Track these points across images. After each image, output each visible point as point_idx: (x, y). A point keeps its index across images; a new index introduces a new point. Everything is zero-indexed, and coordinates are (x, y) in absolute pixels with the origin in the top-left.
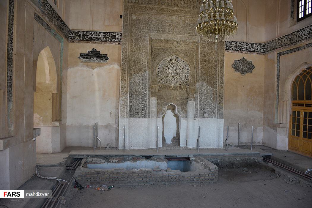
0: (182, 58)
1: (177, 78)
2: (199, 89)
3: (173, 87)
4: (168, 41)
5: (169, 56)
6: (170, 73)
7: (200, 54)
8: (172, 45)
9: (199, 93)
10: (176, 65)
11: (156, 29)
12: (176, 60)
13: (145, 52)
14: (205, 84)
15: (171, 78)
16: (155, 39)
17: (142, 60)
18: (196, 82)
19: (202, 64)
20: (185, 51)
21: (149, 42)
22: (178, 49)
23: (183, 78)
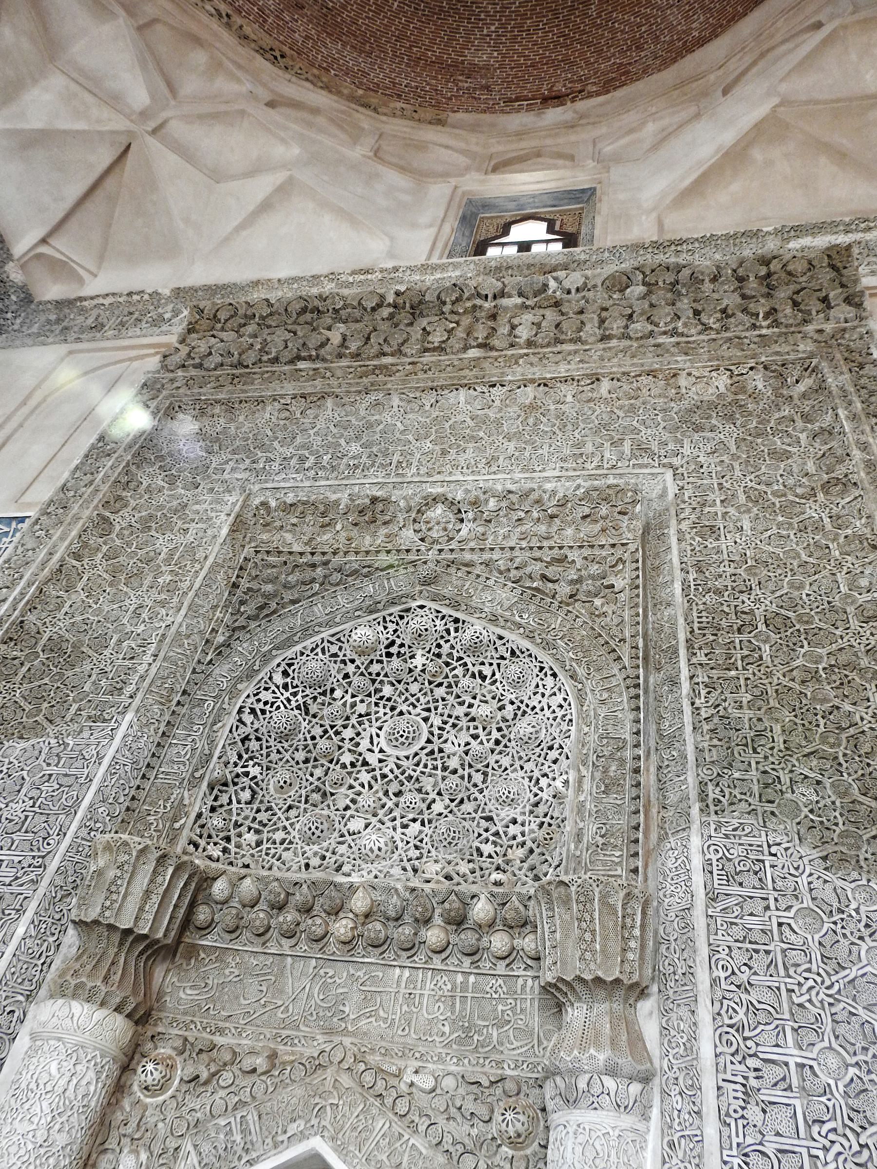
0: (494, 619)
1: (438, 807)
2: (699, 921)
3: (359, 903)
4: (380, 506)
5: (371, 612)
6: (372, 759)
7: (678, 574)
8: (408, 537)
9: (703, 978)
10: (440, 692)
11: (307, 465)
13: (171, 588)
14: (795, 860)
15: (367, 799)
16: (273, 504)
17: (120, 642)
18: (663, 838)
19: (711, 645)
20: (528, 570)
21: (225, 531)
22: (467, 556)
23: (507, 813)
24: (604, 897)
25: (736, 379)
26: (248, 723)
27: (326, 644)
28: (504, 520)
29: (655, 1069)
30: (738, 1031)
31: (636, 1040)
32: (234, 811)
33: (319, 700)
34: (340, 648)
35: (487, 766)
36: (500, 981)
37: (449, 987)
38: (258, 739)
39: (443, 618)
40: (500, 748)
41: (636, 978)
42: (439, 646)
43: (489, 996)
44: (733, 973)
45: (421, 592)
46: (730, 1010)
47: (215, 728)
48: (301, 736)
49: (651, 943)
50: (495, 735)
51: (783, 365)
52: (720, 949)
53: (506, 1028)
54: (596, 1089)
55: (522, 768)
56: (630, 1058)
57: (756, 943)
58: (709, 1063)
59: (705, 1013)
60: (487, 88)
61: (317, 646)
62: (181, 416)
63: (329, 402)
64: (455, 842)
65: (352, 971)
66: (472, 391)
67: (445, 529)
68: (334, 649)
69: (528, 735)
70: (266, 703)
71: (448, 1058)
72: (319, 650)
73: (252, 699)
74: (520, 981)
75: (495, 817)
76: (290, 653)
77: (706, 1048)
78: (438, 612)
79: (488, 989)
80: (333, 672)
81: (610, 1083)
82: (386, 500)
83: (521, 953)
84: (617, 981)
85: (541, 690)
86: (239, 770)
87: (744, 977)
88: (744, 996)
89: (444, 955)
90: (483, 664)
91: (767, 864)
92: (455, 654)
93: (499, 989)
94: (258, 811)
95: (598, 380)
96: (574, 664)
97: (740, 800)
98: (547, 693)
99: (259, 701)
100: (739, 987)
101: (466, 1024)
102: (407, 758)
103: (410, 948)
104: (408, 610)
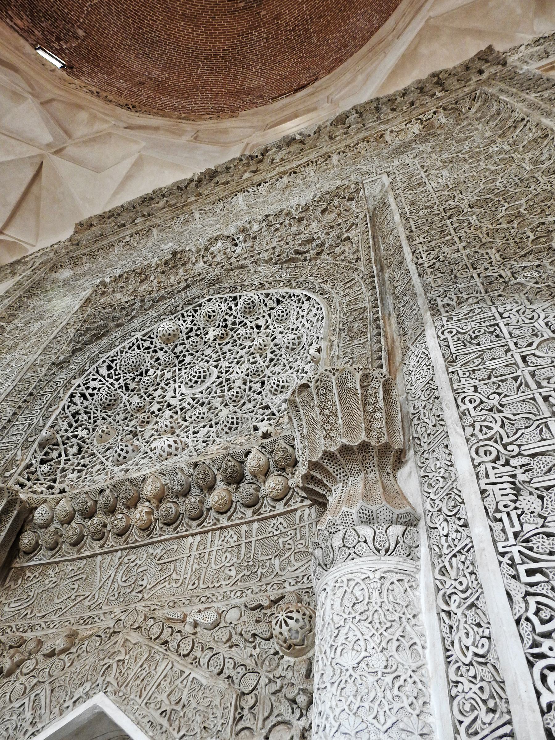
2: (442, 380)
4: (179, 256)
12: (230, 320)
24: (342, 384)
25: (425, 123)
26: (79, 404)
27: (140, 342)
28: (266, 234)
29: (420, 515)
30: (496, 442)
31: (394, 495)
32: (63, 462)
33: (137, 380)
34: (152, 343)
35: (264, 377)
36: (281, 520)
37: (235, 538)
38: (86, 413)
39: (226, 300)
40: (275, 362)
41: (385, 439)
42: (225, 320)
43: (271, 534)
44: (482, 402)
45: (209, 291)
46: (484, 429)
47: (50, 410)
48: (122, 405)
49: (399, 416)
50: (270, 356)
51: (456, 103)
52: (465, 390)
53: (287, 555)
54: (352, 540)
55: (291, 368)
56: (384, 503)
57: (502, 375)
58: (467, 474)
59: (457, 440)
60: (261, 97)
61: (133, 344)
62: (62, 270)
63: (155, 231)
64: (234, 426)
65: (151, 551)
66: (246, 193)
67: (225, 253)
68: (147, 344)
69: (291, 341)
70: (94, 389)
71: (232, 595)
72: (135, 347)
73: (83, 387)
74: (299, 513)
75: (270, 404)
76: (112, 353)
77: (463, 465)
78: (221, 298)
79: (270, 529)
80: (147, 360)
81: (366, 531)
82: (183, 252)
83: (296, 489)
84: (365, 446)
85: (301, 313)
86: (69, 434)
87: (495, 402)
88: (497, 416)
89: (229, 514)
90: (258, 318)
91: (502, 325)
92: (237, 320)
93: (280, 526)
94: (83, 457)
95: (329, 157)
96: (322, 285)
97: (467, 299)
98: (305, 314)
99: (88, 388)
100: (491, 410)
101: (251, 563)
102: (202, 393)
103: (198, 516)
104: (200, 305)
